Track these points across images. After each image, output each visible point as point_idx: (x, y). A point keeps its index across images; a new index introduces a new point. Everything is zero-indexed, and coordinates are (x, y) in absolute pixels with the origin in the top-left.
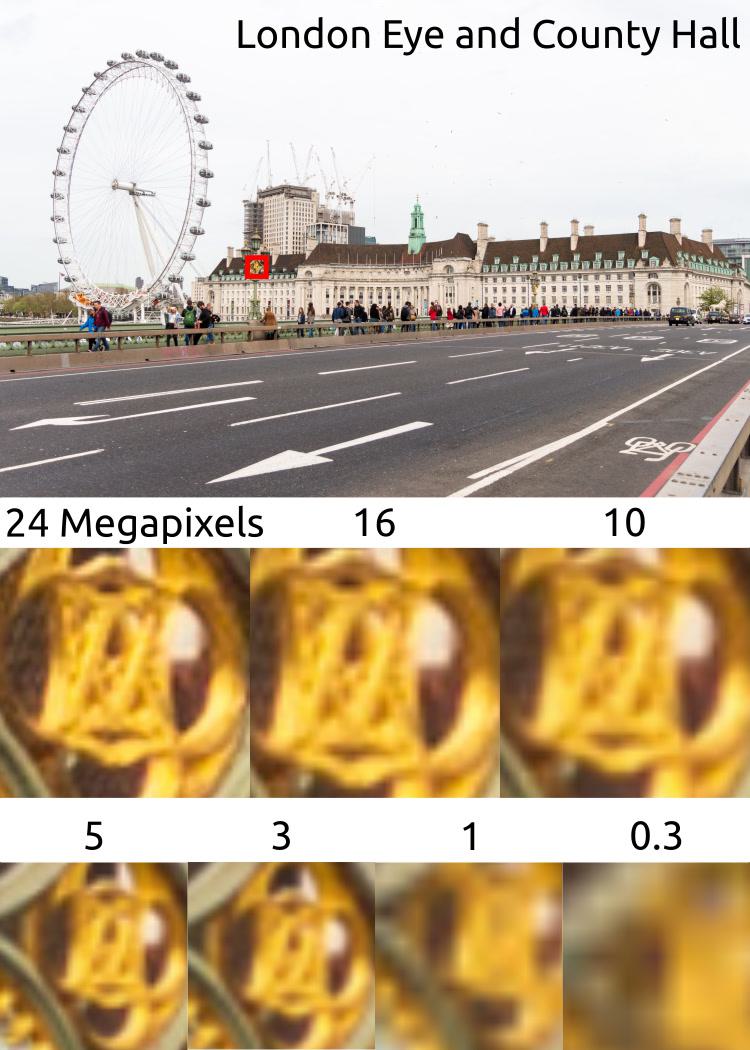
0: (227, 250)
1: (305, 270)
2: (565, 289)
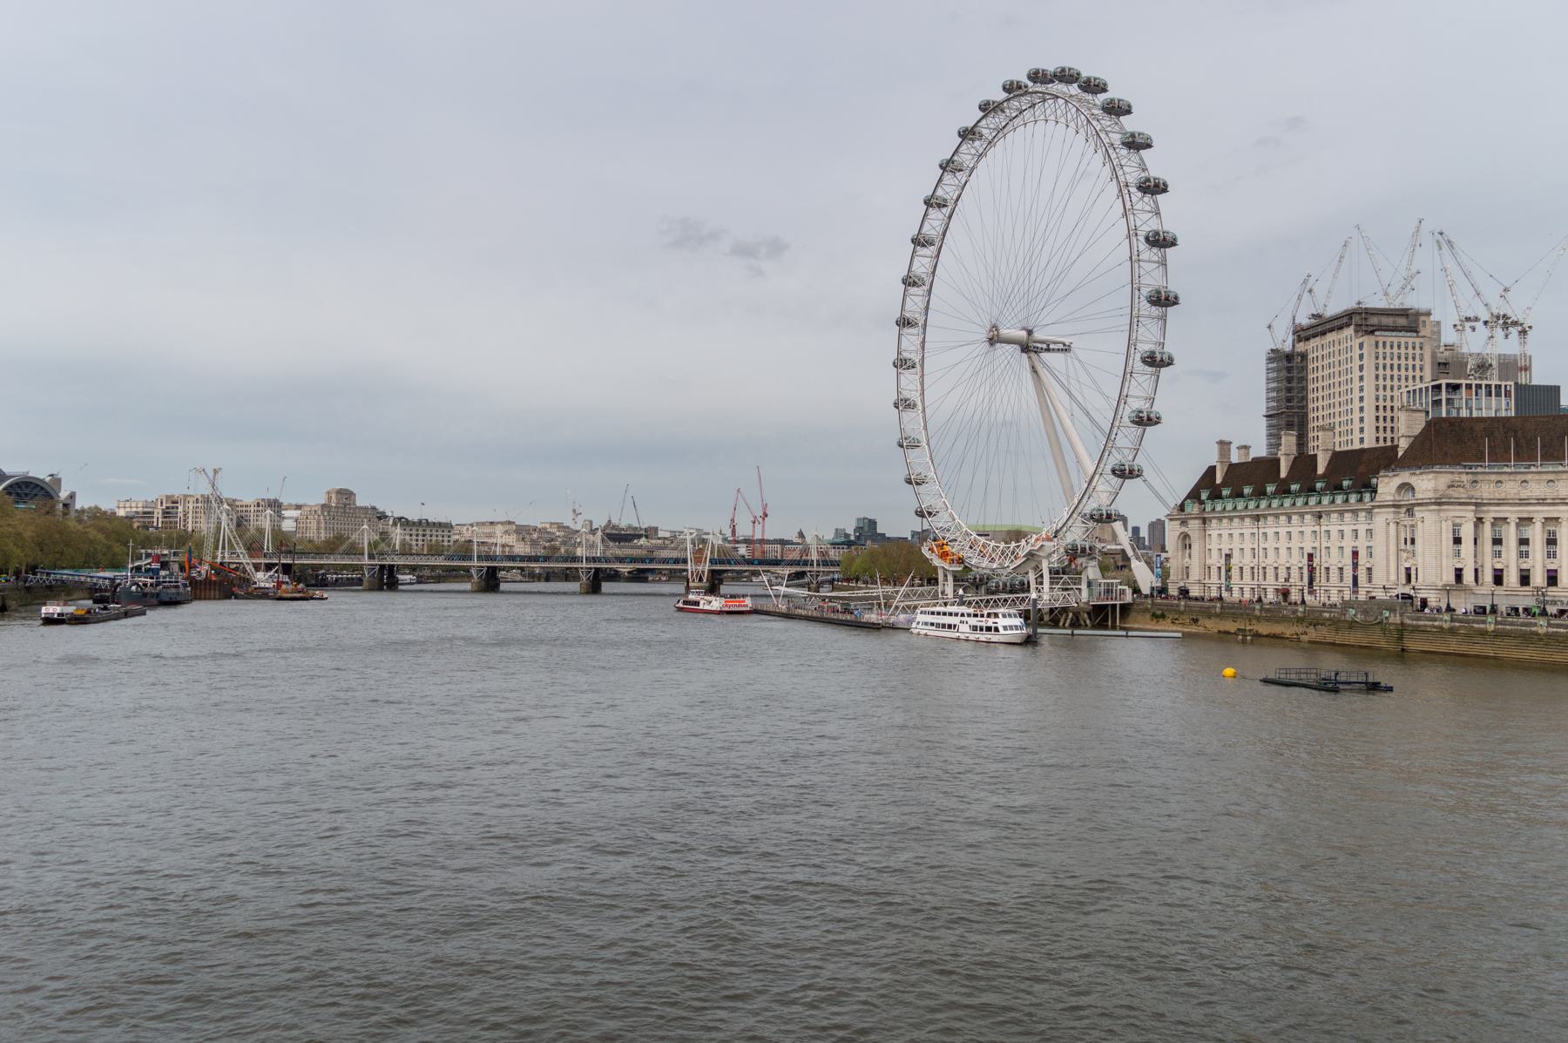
0: (1216, 448)
1: (1398, 481)
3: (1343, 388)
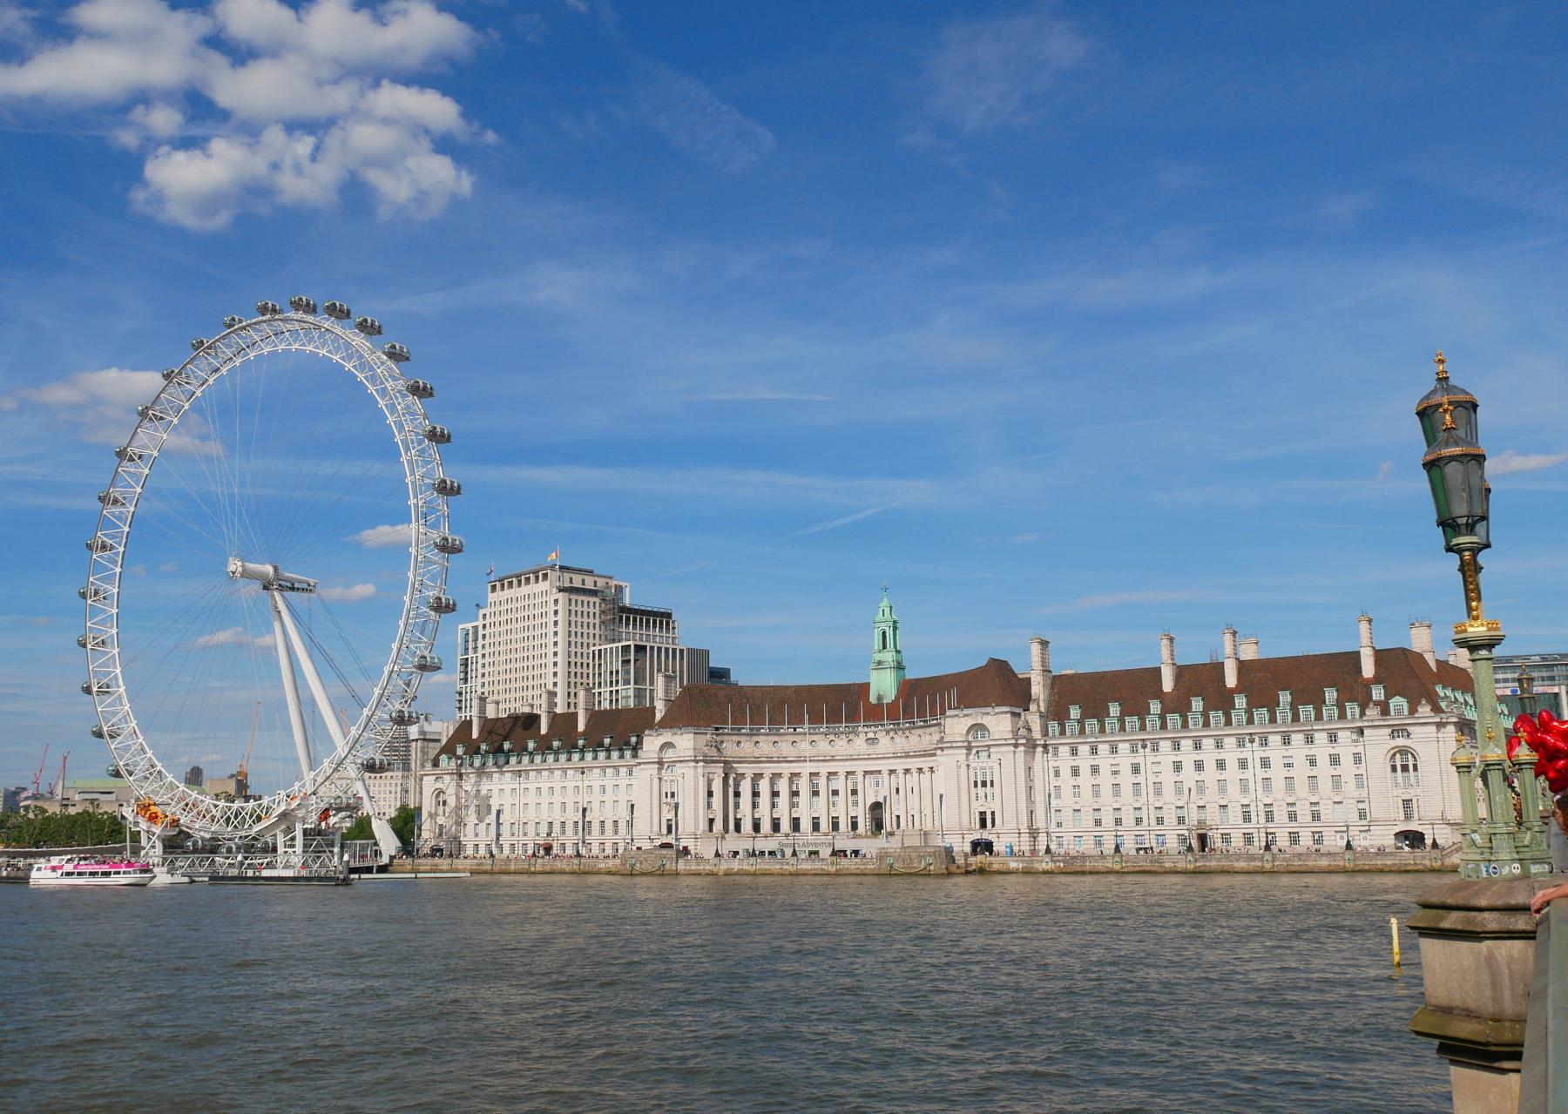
1: (661, 740)
2: (1221, 765)
3: (537, 642)
